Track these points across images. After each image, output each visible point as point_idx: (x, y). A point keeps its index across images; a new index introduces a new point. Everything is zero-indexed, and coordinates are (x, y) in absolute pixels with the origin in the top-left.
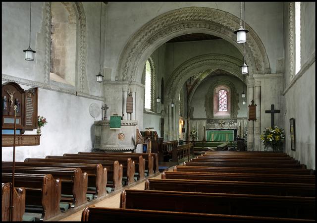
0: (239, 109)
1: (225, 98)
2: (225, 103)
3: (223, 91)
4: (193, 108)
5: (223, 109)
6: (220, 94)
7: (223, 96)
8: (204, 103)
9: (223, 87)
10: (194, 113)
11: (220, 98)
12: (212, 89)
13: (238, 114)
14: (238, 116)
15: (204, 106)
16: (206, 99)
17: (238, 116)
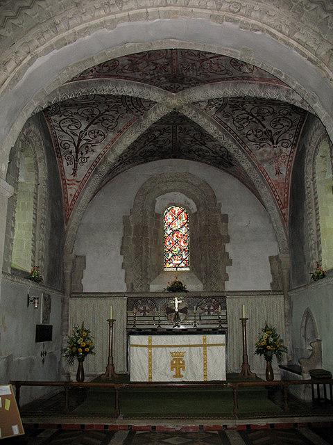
0: (230, 263)
1: (184, 231)
2: (184, 246)
3: (177, 210)
4: (84, 257)
5: (177, 266)
6: (169, 218)
7: (178, 224)
8: (118, 243)
9: (181, 197)
10: (86, 272)
11: (169, 232)
12: (147, 194)
13: (227, 279)
14: (229, 286)
15: (118, 249)
16: (126, 230)
17: (229, 286)
